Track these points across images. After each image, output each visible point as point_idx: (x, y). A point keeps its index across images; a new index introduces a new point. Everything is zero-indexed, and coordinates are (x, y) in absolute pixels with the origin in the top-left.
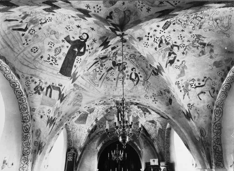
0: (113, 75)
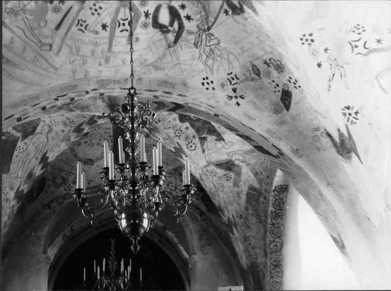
0: (99, 14)
